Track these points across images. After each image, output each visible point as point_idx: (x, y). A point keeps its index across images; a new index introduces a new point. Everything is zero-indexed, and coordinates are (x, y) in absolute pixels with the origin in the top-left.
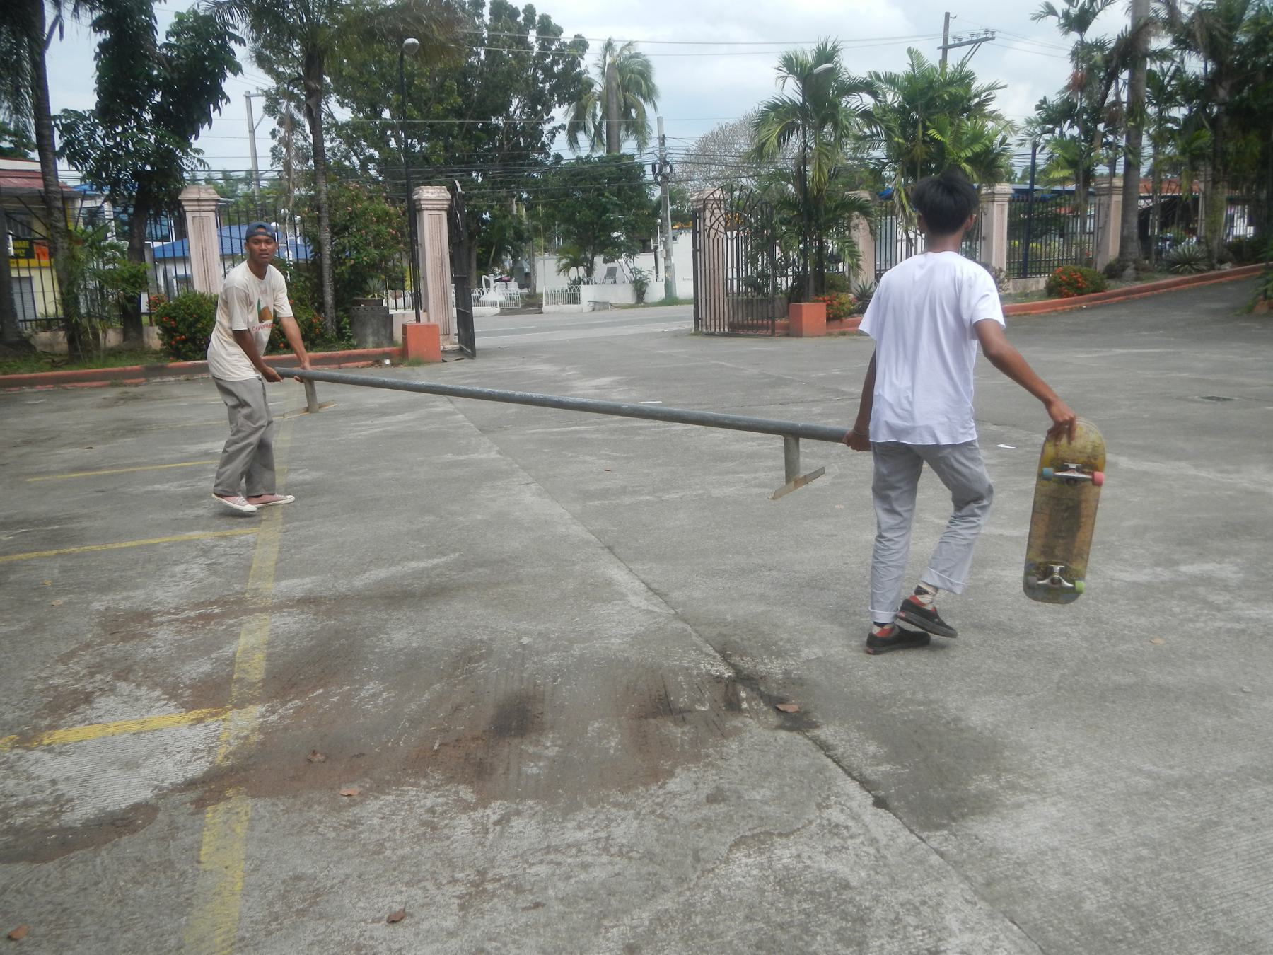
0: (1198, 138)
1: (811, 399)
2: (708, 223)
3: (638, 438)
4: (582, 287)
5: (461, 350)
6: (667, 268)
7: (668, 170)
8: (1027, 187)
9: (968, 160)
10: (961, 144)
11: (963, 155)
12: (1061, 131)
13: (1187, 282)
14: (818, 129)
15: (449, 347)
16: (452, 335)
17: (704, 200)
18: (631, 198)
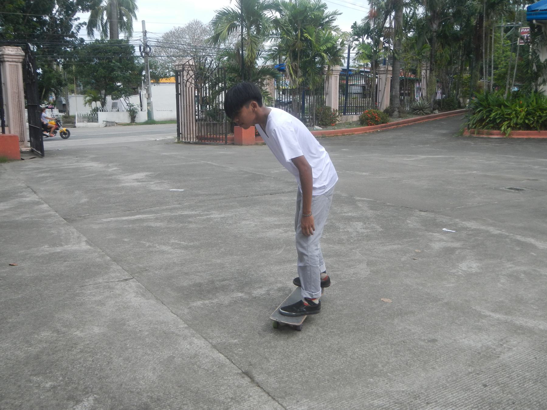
0: (425, 48)
1: (286, 190)
2: (185, 78)
3: (192, 226)
4: (99, 113)
5: (32, 151)
6: (149, 104)
7: (148, 49)
8: (346, 68)
9: (325, 51)
10: (320, 42)
11: (322, 48)
12: (363, 39)
13: (423, 119)
14: (249, 28)
15: (24, 149)
16: (26, 142)
17: (183, 65)
18: (128, 64)
